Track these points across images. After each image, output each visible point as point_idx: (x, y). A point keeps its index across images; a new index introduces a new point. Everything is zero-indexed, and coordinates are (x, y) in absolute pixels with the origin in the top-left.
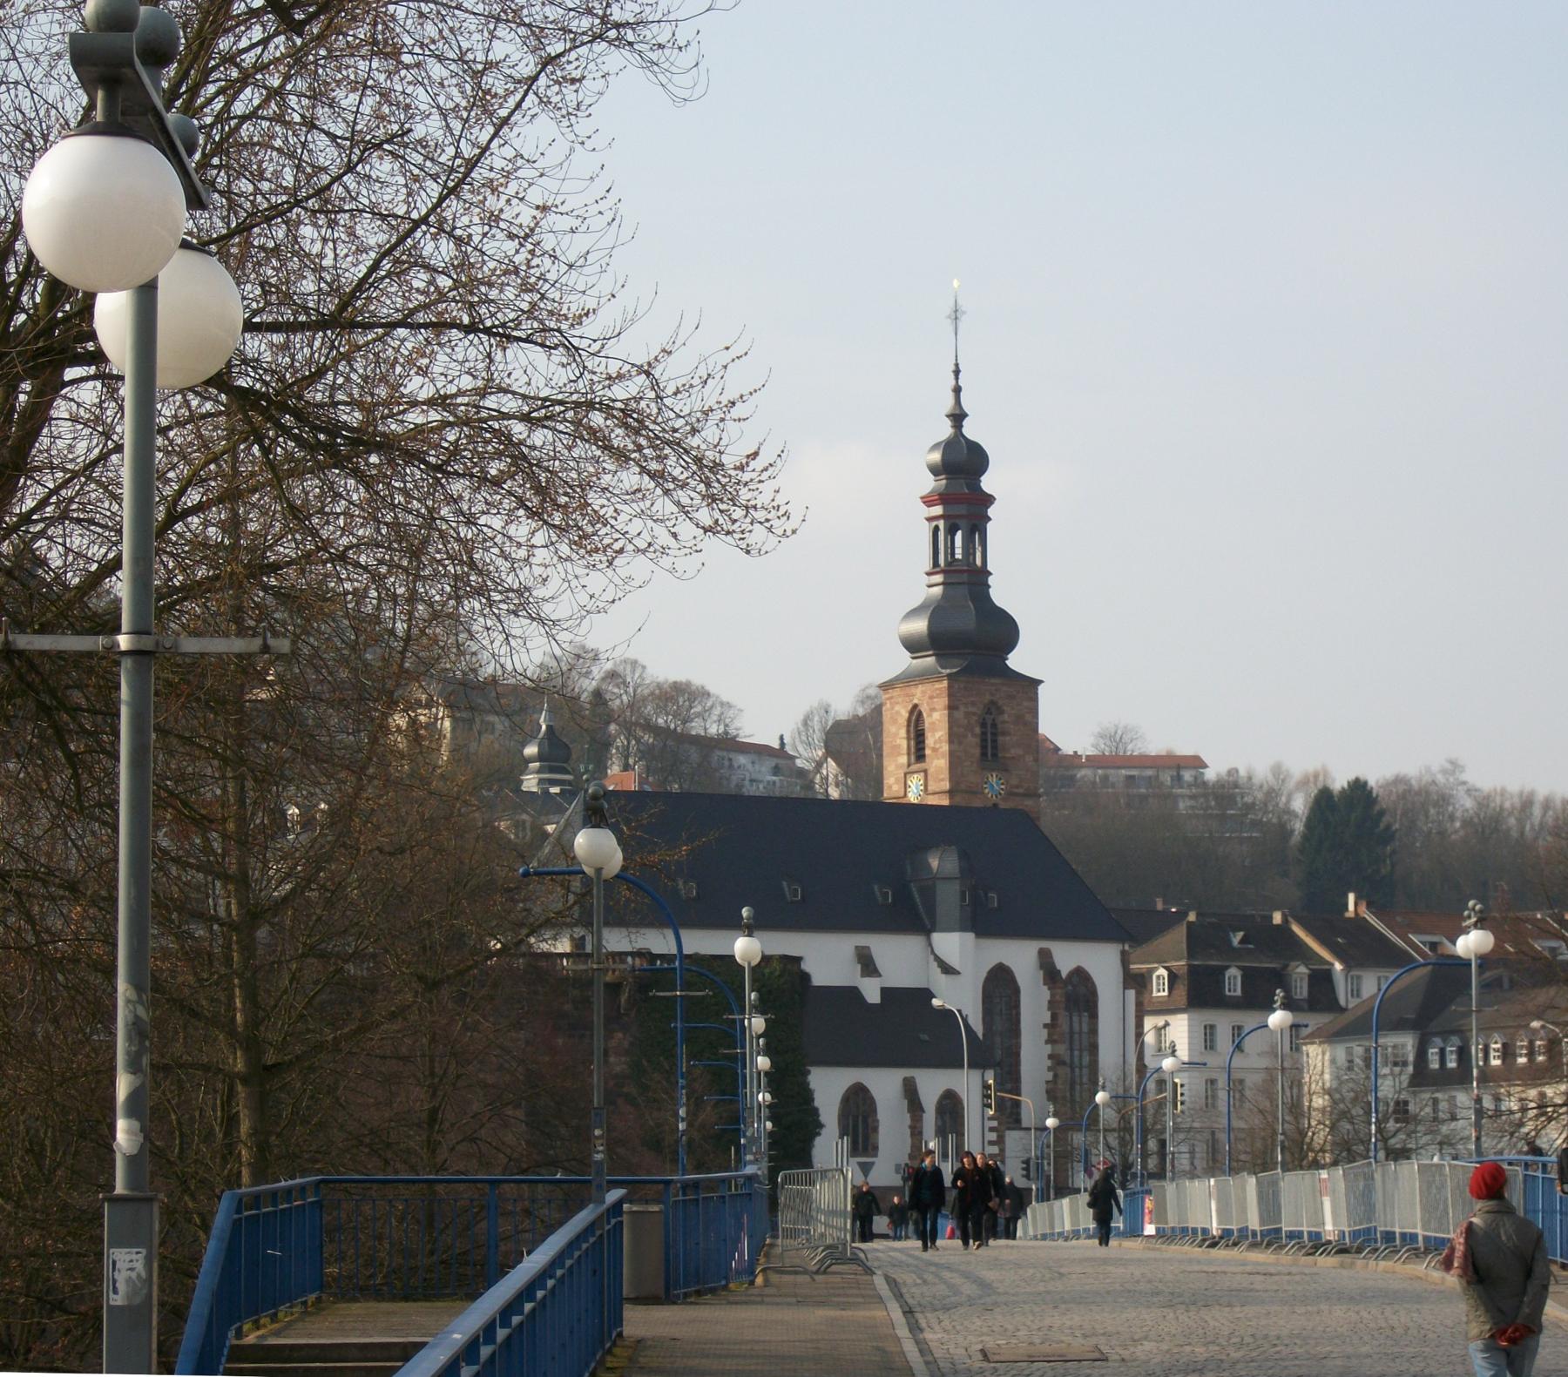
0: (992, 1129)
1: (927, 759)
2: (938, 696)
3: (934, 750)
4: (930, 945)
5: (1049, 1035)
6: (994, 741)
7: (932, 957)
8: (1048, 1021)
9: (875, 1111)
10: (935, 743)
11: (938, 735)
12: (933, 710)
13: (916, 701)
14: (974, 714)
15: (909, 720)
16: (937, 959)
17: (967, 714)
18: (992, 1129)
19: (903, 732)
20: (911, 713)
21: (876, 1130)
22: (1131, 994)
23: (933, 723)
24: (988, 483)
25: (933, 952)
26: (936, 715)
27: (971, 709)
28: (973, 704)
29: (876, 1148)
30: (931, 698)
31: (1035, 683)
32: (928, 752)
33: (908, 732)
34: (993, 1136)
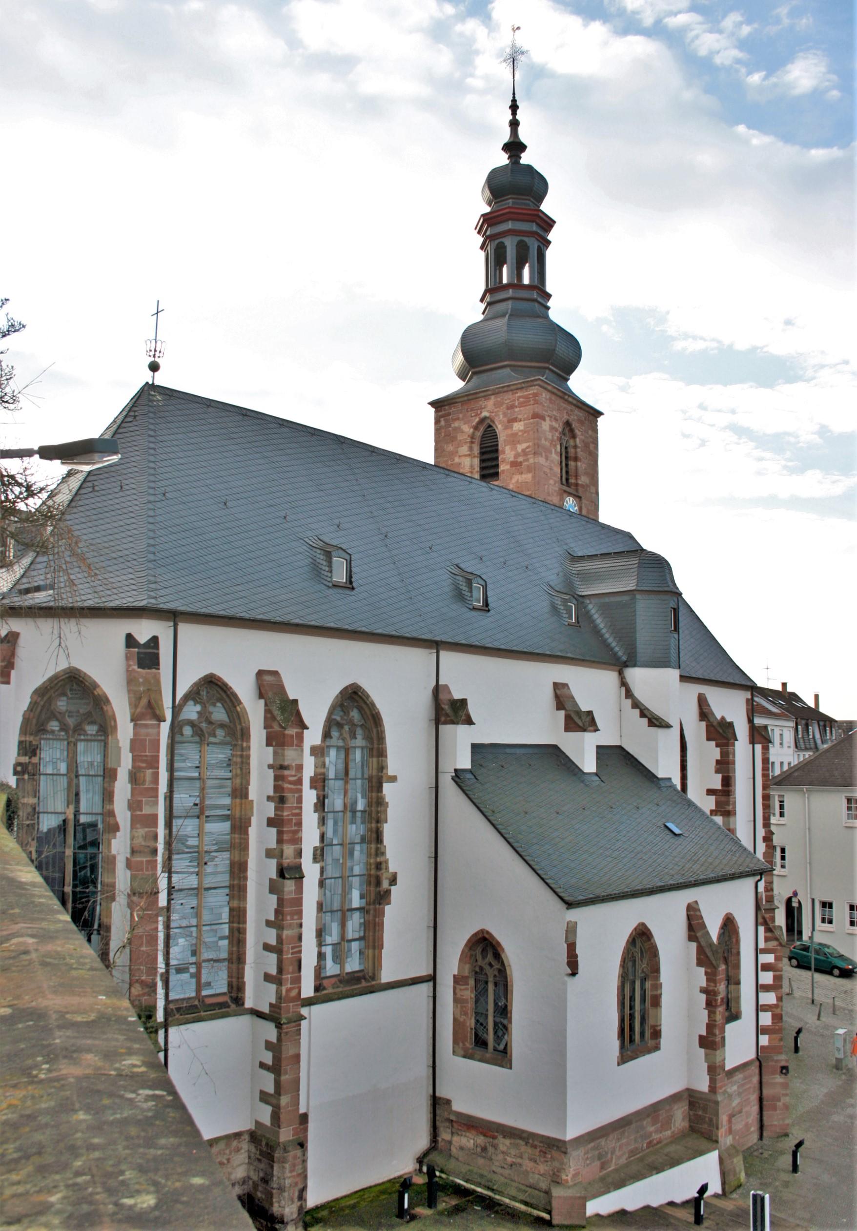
0: (766, 967)
1: (501, 477)
2: (521, 405)
3: (515, 464)
4: (624, 683)
5: (718, 803)
6: (567, 465)
7: (629, 702)
8: (718, 786)
9: (656, 970)
10: (517, 456)
11: (520, 448)
12: (515, 420)
13: (485, 414)
14: (556, 430)
15: (472, 437)
16: (636, 705)
17: (552, 428)
18: (766, 967)
19: (464, 450)
20: (476, 428)
21: (656, 1002)
22: (758, 748)
23: (515, 435)
24: (547, 207)
25: (629, 694)
26: (518, 426)
27: (554, 424)
28: (556, 420)
29: (657, 1034)
30: (511, 407)
31: (599, 414)
32: (503, 467)
33: (471, 449)
34: (767, 978)
